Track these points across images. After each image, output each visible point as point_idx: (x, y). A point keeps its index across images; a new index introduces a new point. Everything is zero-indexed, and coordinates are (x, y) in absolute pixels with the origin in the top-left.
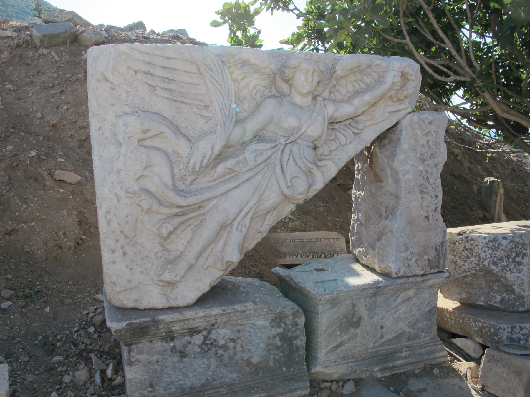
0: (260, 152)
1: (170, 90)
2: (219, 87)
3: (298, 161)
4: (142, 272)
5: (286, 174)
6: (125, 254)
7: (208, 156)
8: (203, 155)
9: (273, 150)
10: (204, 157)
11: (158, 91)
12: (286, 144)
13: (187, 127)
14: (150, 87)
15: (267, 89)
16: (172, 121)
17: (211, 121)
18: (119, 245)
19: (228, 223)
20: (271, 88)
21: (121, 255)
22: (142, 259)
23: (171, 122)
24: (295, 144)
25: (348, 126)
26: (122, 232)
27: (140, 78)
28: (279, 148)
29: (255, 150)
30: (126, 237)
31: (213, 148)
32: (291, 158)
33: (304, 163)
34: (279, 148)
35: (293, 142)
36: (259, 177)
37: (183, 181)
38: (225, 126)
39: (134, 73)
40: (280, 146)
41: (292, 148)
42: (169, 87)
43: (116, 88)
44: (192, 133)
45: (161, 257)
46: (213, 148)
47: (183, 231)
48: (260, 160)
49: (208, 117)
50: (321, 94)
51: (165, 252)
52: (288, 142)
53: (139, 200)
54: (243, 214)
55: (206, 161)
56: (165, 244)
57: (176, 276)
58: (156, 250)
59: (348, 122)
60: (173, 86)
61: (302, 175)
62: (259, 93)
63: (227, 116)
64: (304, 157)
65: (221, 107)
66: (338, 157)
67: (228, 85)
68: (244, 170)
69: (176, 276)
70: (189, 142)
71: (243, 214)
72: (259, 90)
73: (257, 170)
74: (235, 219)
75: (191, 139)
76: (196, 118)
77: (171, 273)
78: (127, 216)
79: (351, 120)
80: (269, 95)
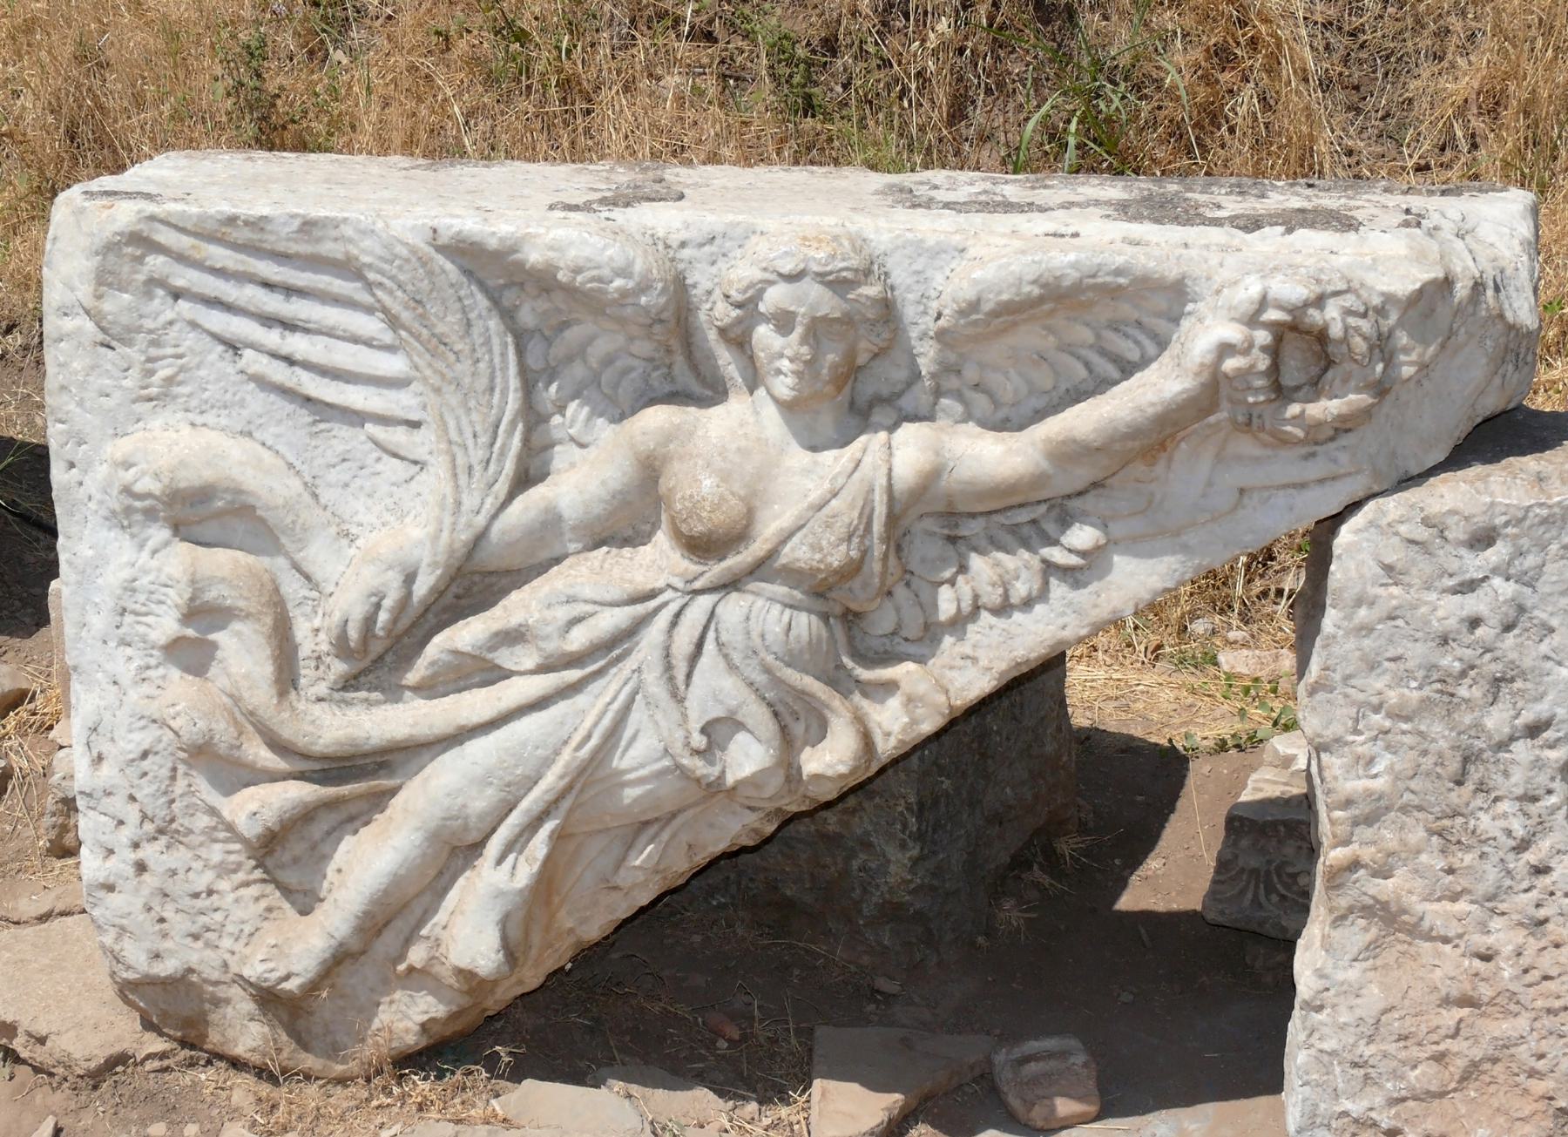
0: (589, 608)
1: (290, 361)
2: (452, 357)
3: (737, 658)
4: (196, 937)
5: (687, 704)
6: (141, 867)
7: (388, 603)
8: (374, 599)
9: (640, 609)
10: (378, 606)
11: (252, 360)
12: (697, 592)
13: (346, 485)
14: (221, 348)
15: (656, 368)
16: (297, 464)
17: (424, 476)
18: (126, 834)
19: (473, 836)
20: (670, 366)
21: (131, 871)
22: (196, 896)
23: (291, 466)
24: (734, 595)
25: (1026, 530)
26: (132, 798)
27: (189, 316)
28: (665, 604)
29: (571, 600)
30: (144, 817)
31: (410, 579)
32: (710, 646)
33: (767, 670)
34: (665, 604)
35: (724, 586)
36: (581, 700)
37: (322, 668)
38: (458, 503)
39: (170, 300)
40: (668, 595)
41: (719, 610)
42: (285, 351)
43: (114, 343)
44: (362, 509)
45: (257, 899)
46: (410, 579)
47: (329, 833)
48: (578, 639)
49: (416, 463)
50: (899, 395)
51: (270, 888)
52: (697, 585)
53: (172, 711)
54: (515, 819)
55: (383, 617)
56: (269, 862)
57: (287, 978)
58: (241, 876)
59: (1023, 516)
60: (297, 344)
61: (757, 714)
62: (624, 383)
63: (478, 468)
64: (767, 648)
65: (454, 435)
66: (968, 650)
67: (490, 351)
68: (529, 662)
69: (287, 978)
70: (345, 542)
71: (515, 819)
72: (626, 371)
73: (573, 675)
74: (494, 830)
75: (354, 530)
76: (379, 459)
77: (271, 965)
78: (145, 755)
79: (1043, 508)
80: (667, 388)
